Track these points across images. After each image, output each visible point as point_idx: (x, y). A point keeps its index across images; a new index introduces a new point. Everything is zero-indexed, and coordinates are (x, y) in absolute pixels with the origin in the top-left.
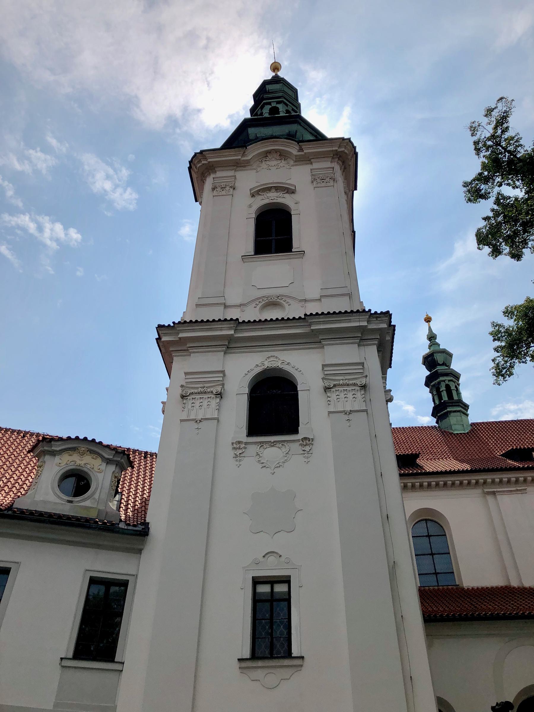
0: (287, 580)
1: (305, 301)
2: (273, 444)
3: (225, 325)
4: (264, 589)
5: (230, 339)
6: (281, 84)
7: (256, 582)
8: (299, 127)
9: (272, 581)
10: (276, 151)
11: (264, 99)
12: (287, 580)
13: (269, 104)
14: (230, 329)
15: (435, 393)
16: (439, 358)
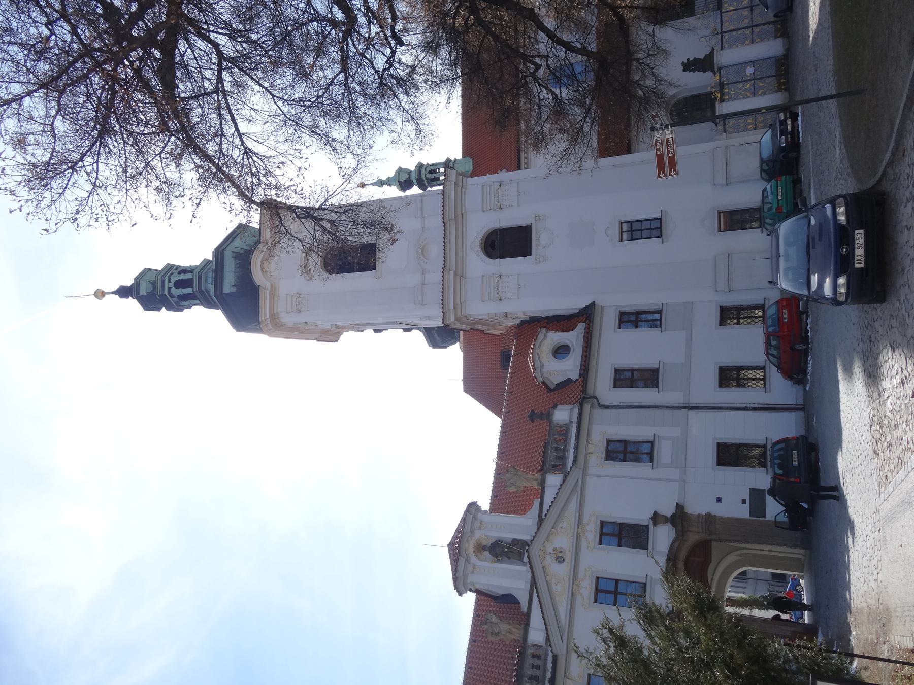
0: (621, 223)
1: (423, 228)
2: (537, 239)
3: (446, 277)
4: (625, 236)
5: (456, 274)
6: (141, 281)
7: (621, 240)
8: (227, 249)
9: (622, 232)
10: (262, 263)
11: (163, 295)
12: (621, 223)
13: (169, 289)
14: (449, 274)
15: (435, 183)
16: (404, 177)
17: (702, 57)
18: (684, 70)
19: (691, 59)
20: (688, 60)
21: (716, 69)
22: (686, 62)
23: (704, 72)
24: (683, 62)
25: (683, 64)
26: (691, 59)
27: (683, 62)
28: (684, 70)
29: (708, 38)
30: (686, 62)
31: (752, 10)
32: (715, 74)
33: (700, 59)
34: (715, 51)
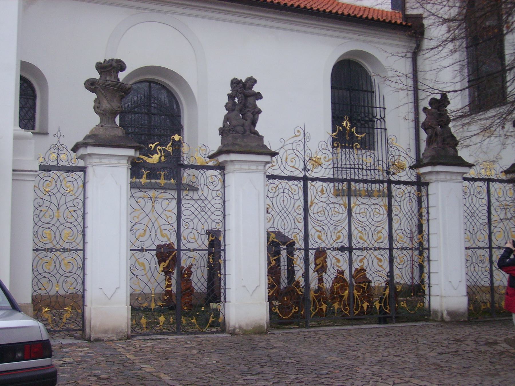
17: (259, 128)
18: (235, 83)
19: (259, 103)
20: (258, 96)
21: (222, 158)
22: (256, 89)
23: (222, 132)
24: (255, 81)
25: (252, 81)
26: (259, 103)
27: (255, 81)
28: (235, 83)
29: (301, 148)
30: (256, 89)
31: (342, 249)
32: (211, 157)
33: (254, 123)
34: (267, 158)
